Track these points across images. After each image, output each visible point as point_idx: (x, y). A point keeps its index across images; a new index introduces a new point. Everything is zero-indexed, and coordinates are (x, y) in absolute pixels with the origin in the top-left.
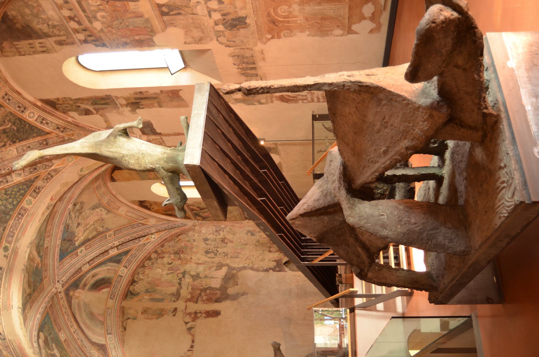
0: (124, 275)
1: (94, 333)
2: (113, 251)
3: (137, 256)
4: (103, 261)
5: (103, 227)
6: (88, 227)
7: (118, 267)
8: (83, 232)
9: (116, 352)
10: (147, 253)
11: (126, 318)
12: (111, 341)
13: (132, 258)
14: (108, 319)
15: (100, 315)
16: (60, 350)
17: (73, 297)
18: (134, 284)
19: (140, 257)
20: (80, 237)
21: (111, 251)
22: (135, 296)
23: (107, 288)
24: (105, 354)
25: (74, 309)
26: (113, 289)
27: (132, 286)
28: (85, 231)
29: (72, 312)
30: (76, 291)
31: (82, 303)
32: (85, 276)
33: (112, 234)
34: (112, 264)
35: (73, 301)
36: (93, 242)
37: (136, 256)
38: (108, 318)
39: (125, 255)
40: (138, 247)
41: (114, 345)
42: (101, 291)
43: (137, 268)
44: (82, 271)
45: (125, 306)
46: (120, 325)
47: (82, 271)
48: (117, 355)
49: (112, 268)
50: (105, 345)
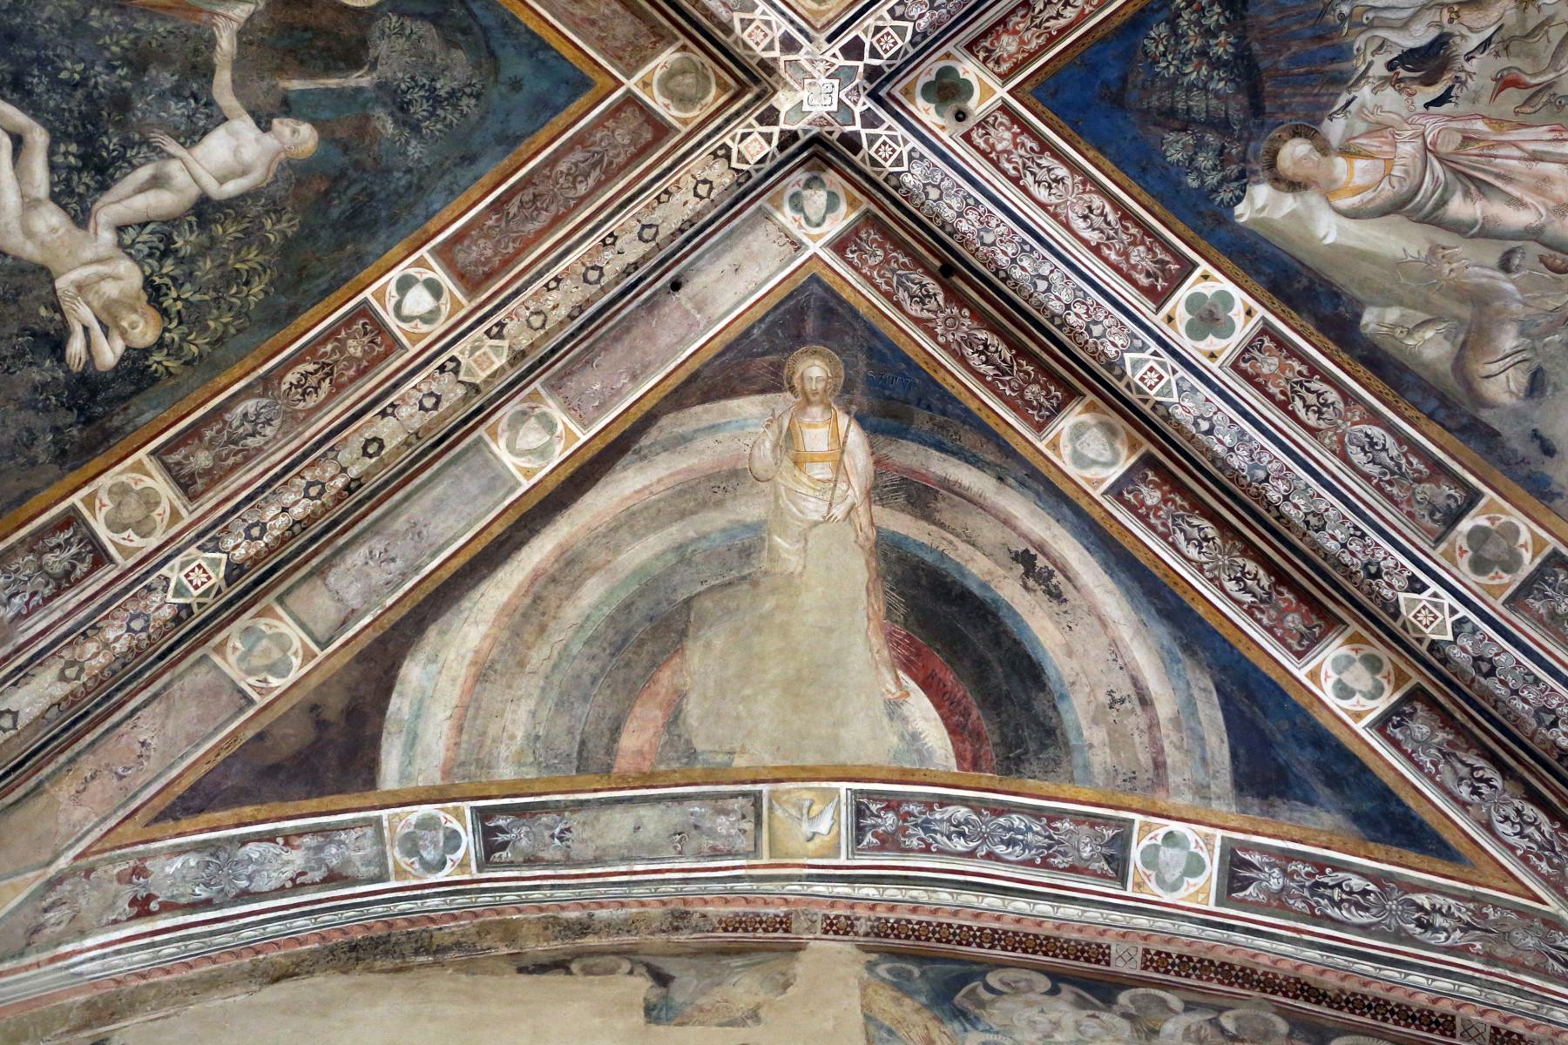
0: (1144, 885)
1: (483, 673)
2: (1347, 678)
3: (1411, 940)
4: (1213, 621)
5: (1536, 385)
6: (1460, 207)
7: (1202, 791)
8: (1387, 191)
9: (281, 891)
10: (1493, 1019)
11: (669, 966)
12: (411, 845)
13: (1358, 901)
14: (644, 812)
15: (674, 717)
16: (274, 230)
17: (783, 401)
18: (1064, 987)
19: (1418, 978)
20: (1328, 194)
21: (1342, 665)
22: (923, 999)
23: (954, 730)
24: (272, 771)
25: (683, 441)
26: (962, 812)
27: (1044, 983)
28: (1397, 207)
29: (649, 420)
30: (843, 420)
31: (749, 510)
32: (1001, 479)
33: (1511, 564)
34: (1211, 715)
35: (748, 407)
36: (1347, 395)
37: (1400, 936)
38: (654, 821)
39: (1357, 818)
40: (1522, 912)
41: (364, 871)
42: (912, 685)
43: (1268, 983)
44: (1039, 428)
45: (803, 966)
46: (591, 941)
47: (1039, 428)
48: (245, 896)
49: (1168, 737)
50: (371, 782)
